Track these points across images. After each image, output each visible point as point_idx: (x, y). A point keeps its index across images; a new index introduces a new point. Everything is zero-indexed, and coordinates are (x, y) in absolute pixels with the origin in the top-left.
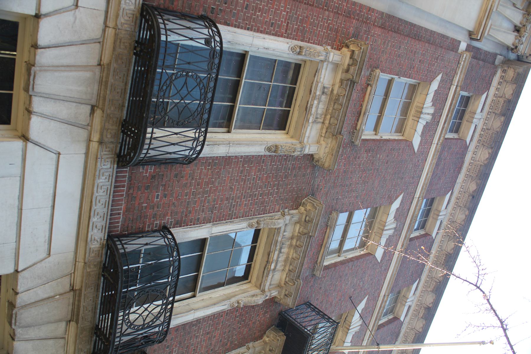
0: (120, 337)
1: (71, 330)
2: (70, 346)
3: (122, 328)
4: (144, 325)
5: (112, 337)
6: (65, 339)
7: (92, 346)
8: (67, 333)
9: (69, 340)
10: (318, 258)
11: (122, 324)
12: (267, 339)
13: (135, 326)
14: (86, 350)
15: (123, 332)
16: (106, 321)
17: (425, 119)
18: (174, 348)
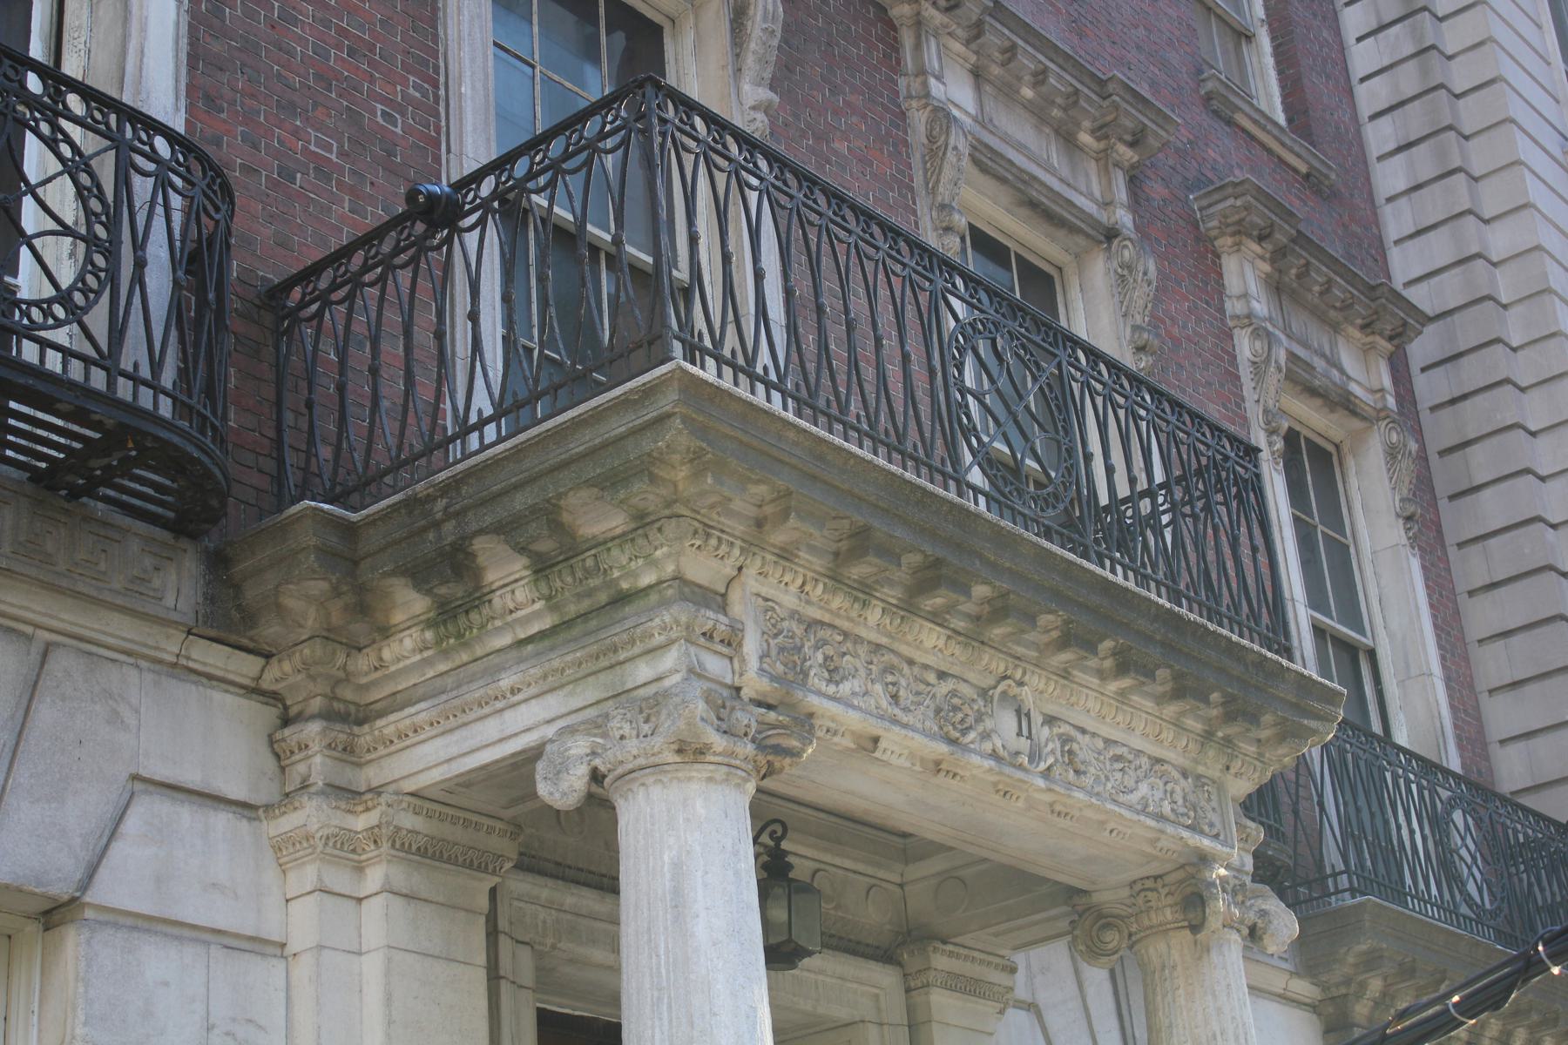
0: (113, 373)
1: (12, 605)
2: (104, 633)
3: (67, 353)
4: (91, 240)
5: (98, 412)
6: (58, 645)
7: (141, 527)
8: (29, 630)
9: (70, 628)
11: (45, 344)
13: (84, 282)
14: (148, 562)
15: (92, 353)
16: (40, 432)
18: (305, 148)
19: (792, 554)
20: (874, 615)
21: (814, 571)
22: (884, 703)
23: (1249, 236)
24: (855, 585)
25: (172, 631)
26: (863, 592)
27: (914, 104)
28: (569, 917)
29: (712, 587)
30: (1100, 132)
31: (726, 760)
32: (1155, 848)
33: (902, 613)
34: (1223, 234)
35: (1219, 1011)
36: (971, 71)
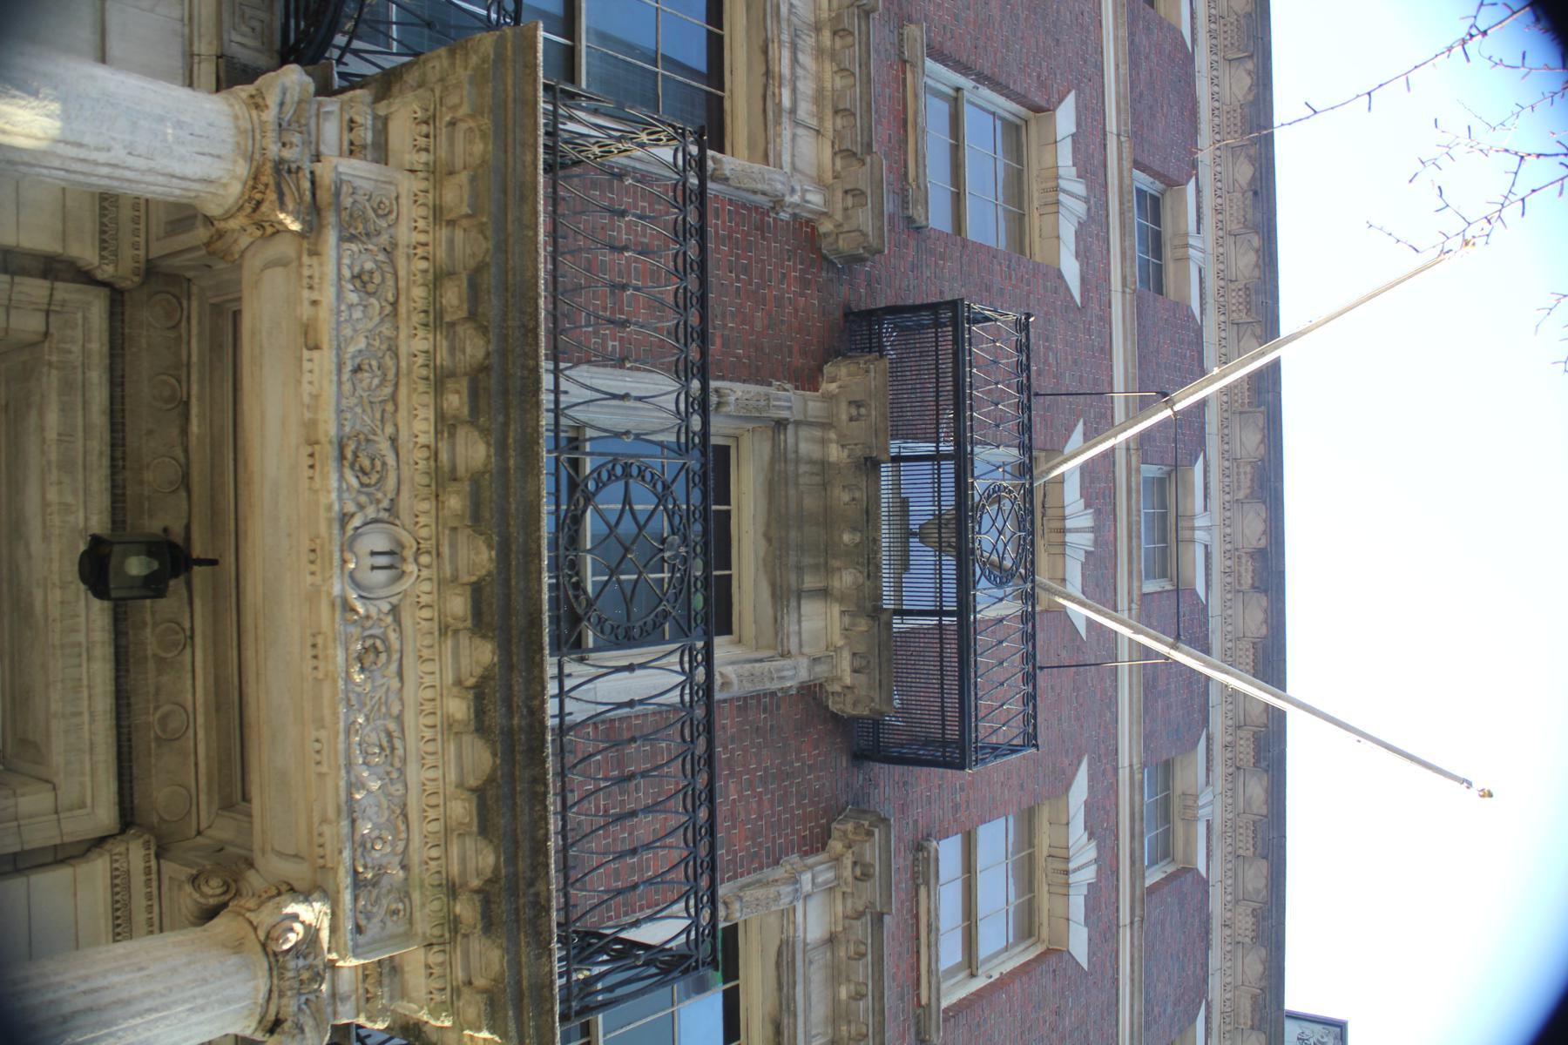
10: (906, 166)
12: (833, 387)
17: (1073, 209)
19: (441, 220)
20: (421, 344)
21: (435, 255)
22: (352, 349)
24: (438, 306)
25: (215, 42)
26: (436, 320)
27: (788, 867)
28: (80, 377)
29: (390, 153)
32: (320, 824)
33: (432, 376)
35: (174, 970)
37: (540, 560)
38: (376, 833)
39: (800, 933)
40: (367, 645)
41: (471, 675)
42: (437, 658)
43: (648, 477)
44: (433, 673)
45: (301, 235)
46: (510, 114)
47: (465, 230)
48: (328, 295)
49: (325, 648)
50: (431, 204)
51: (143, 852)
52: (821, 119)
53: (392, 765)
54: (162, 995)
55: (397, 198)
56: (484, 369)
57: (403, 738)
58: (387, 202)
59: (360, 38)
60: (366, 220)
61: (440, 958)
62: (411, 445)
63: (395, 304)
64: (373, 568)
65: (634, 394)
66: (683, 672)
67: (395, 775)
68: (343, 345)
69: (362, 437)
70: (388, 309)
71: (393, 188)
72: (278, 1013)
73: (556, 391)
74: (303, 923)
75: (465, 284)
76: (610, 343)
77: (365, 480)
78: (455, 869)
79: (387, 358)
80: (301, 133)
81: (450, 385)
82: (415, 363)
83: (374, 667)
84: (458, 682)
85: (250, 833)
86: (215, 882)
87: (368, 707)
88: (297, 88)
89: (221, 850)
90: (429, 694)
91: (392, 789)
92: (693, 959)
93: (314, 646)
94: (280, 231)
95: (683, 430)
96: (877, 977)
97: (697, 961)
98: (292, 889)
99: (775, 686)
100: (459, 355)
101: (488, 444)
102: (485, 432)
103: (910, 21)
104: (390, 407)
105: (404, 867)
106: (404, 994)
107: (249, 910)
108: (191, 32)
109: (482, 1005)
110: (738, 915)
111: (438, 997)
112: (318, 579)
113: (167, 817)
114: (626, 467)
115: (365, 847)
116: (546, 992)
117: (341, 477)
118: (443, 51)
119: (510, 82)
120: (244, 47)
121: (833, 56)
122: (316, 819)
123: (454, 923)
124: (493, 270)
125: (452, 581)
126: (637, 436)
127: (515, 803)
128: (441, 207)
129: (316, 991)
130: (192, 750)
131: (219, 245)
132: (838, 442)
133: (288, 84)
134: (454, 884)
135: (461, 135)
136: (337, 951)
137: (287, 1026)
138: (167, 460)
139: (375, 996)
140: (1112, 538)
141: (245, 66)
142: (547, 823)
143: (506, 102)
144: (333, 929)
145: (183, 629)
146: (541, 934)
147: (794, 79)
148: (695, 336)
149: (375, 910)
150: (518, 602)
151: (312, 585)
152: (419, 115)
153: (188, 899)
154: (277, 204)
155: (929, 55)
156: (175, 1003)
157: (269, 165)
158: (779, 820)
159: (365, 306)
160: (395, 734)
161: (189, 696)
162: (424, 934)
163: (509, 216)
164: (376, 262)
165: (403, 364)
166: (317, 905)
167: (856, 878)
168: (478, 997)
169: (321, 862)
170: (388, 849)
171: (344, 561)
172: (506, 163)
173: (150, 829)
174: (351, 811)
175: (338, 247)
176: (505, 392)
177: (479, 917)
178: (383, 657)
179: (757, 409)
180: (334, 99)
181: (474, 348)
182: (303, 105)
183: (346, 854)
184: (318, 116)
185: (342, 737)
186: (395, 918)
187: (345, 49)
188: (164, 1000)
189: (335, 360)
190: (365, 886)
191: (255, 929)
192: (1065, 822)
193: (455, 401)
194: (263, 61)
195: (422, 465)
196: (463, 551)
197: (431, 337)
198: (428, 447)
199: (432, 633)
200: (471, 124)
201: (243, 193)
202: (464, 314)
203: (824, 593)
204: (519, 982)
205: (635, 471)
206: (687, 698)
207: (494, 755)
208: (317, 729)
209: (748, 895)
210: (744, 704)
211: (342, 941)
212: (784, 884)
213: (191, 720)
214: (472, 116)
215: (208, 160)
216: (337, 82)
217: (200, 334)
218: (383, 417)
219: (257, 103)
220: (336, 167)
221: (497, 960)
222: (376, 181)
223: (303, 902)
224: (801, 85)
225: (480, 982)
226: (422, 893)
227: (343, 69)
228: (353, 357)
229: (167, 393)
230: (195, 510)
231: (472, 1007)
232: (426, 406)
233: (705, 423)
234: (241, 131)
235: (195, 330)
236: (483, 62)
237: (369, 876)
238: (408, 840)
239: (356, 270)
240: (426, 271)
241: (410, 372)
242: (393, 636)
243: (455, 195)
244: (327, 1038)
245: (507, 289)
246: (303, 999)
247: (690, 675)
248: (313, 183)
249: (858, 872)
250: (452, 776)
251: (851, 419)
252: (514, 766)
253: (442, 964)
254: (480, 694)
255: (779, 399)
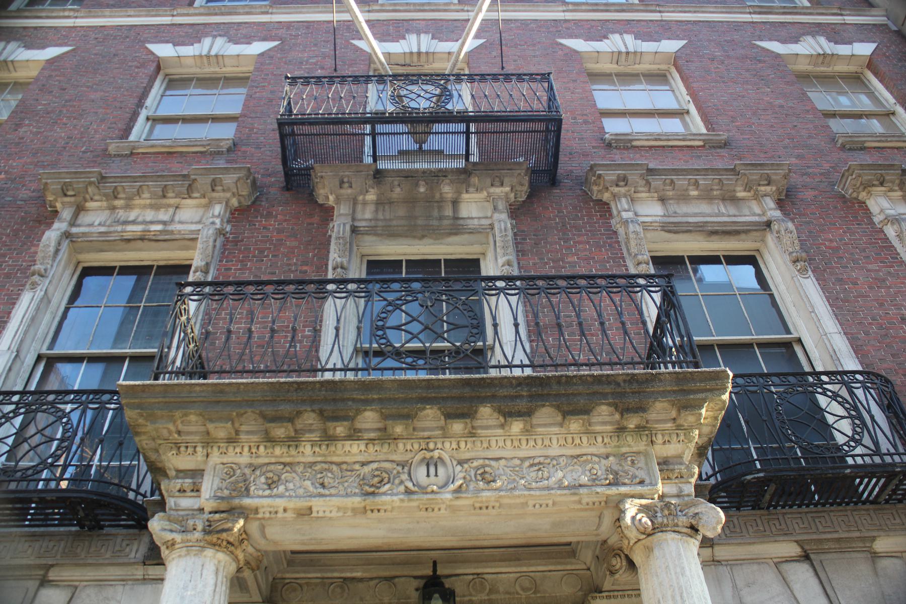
2: (109, 576)
9: (92, 578)
10: (196, 153)
12: (331, 198)
19: (236, 439)
20: (307, 449)
22: (311, 489)
23: (874, 185)
25: (136, 567)
26: (293, 441)
27: (618, 226)
29: (198, 468)
30: (748, 188)
31: (184, 545)
32: (582, 504)
33: (326, 443)
34: (859, 193)
35: (661, 584)
36: (659, 200)
37: (432, 380)
38: (588, 473)
39: (658, 219)
40: (480, 479)
41: (498, 419)
42: (488, 439)
43: (384, 315)
44: (497, 441)
45: (246, 519)
46: (172, 400)
47: (241, 425)
48: (280, 503)
49: (482, 502)
50: (226, 444)
51: (598, 600)
52: (169, 206)
53: (549, 464)
54: (674, 590)
55: (223, 464)
56: (321, 413)
57: (534, 457)
58: (226, 470)
59: (130, 484)
60: (237, 482)
61: (660, 436)
62: (366, 454)
63: (285, 464)
64: (436, 475)
65: (335, 324)
66: (498, 294)
67: (555, 462)
68: (309, 494)
69: (361, 482)
70: (288, 468)
71: (218, 467)
72: (687, 527)
73: (334, 370)
74: (637, 514)
75: (273, 425)
76: (307, 333)
77: (386, 480)
78: (609, 428)
79: (316, 468)
80: (187, 520)
81: (331, 432)
82: (318, 452)
83: (493, 474)
84: (502, 426)
85: (588, 543)
86: (614, 562)
87: (516, 477)
88: (162, 522)
89: (597, 557)
90: (509, 443)
91: (563, 464)
92: (666, 289)
93: (481, 508)
94: (244, 530)
95: (357, 294)
96: (685, 173)
97: (668, 287)
98: (618, 519)
99: (510, 233)
100: (313, 427)
101: (365, 410)
102: (358, 412)
103: (106, 150)
104: (344, 467)
105: (607, 457)
106: (680, 457)
107: (629, 543)
108: (130, 580)
109: (687, 413)
110: (645, 257)
111: (682, 438)
112: (443, 507)
113: (580, 587)
114: (378, 328)
115: (595, 479)
116: (681, 376)
117: (384, 494)
118: (137, 439)
119: (153, 400)
120: (138, 550)
121: (130, 198)
122: (579, 506)
123: (640, 429)
124: (264, 408)
125: (444, 430)
126: (360, 322)
127: (572, 394)
128: (227, 439)
129: (675, 506)
130: (541, 573)
131: (253, 564)
132: (365, 195)
133: (160, 528)
134: (618, 428)
135: (185, 427)
136: (654, 494)
137: (694, 523)
138: (377, 590)
139: (680, 473)
140: (424, 22)
141: (149, 549)
142: (584, 375)
143: (166, 402)
144: (641, 497)
145: (473, 579)
146: (647, 379)
147: (144, 223)
148: (300, 287)
149: (631, 473)
150: (456, 392)
151: (446, 510)
152: (174, 452)
153: (623, 576)
154: (228, 533)
155: (127, 138)
156: (678, 583)
157: (207, 537)
158: (590, 231)
159: (287, 481)
160: (531, 462)
161: (512, 575)
162: (645, 445)
163: (233, 399)
164: (260, 476)
165: (319, 459)
166: (627, 506)
167: (626, 185)
168: (682, 415)
169: (603, 504)
170: (596, 466)
171: (433, 492)
172: (202, 402)
173: (586, 595)
174: (574, 487)
175: (252, 497)
176: (334, 400)
177: (636, 415)
178: (487, 469)
179: (345, 245)
180: (167, 501)
181: (309, 419)
182: (171, 519)
183: (599, 490)
184: (177, 510)
185: (532, 493)
186: (636, 462)
187: (137, 492)
188: (677, 589)
189: (317, 498)
190: (617, 479)
191: (639, 540)
192: (597, 54)
193: (340, 429)
194: (146, 539)
195: (377, 448)
196: (428, 424)
197: (303, 443)
198: (367, 444)
199: (474, 441)
200: (179, 422)
201: (223, 552)
202: (290, 425)
203: (455, 203)
204: (674, 392)
205: (380, 323)
206: (513, 292)
207: (544, 406)
208: (528, 506)
209: (634, 250)
210: (520, 252)
211: (648, 492)
212: (628, 229)
213: (524, 574)
214: (174, 422)
215: (205, 572)
216: (156, 497)
217: (305, 572)
218: (350, 471)
219: (171, 545)
220: (207, 499)
221: (662, 404)
222: (214, 476)
223: (625, 514)
224: (148, 219)
225: (674, 414)
226: (622, 447)
227: (148, 494)
228: (316, 488)
229: (338, 590)
230: (406, 573)
231: (688, 419)
232: (343, 445)
233: (353, 281)
234: (188, 554)
235: (302, 575)
236: (142, 416)
237: (611, 476)
238: (592, 455)
239: (266, 487)
240: (265, 447)
241: (324, 455)
242: (475, 464)
243: (220, 431)
244: (702, 500)
245: (275, 400)
246: (679, 513)
247: (501, 290)
248: (216, 512)
249: (622, 183)
250: (556, 429)
251: (351, 187)
252: (550, 394)
253: (663, 435)
254: (508, 414)
255: (339, 231)
